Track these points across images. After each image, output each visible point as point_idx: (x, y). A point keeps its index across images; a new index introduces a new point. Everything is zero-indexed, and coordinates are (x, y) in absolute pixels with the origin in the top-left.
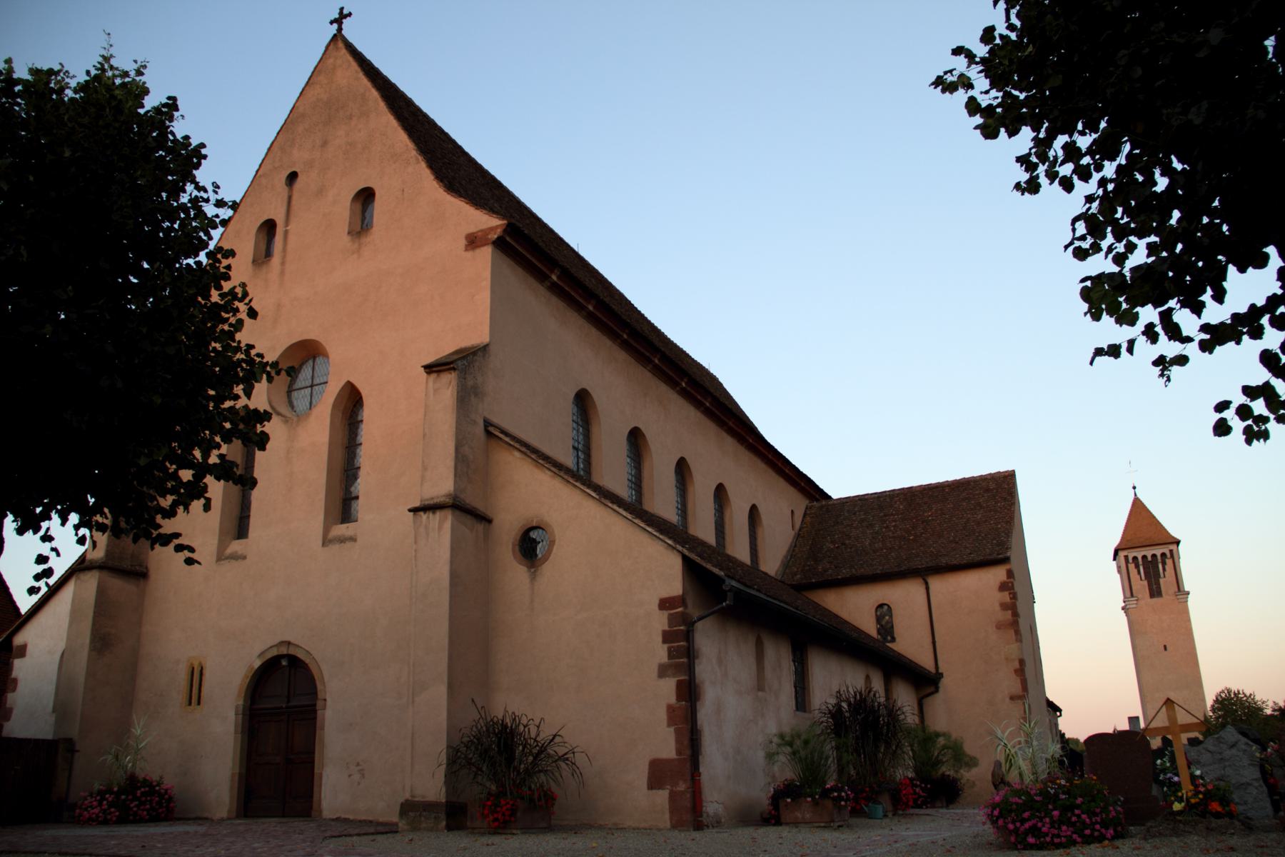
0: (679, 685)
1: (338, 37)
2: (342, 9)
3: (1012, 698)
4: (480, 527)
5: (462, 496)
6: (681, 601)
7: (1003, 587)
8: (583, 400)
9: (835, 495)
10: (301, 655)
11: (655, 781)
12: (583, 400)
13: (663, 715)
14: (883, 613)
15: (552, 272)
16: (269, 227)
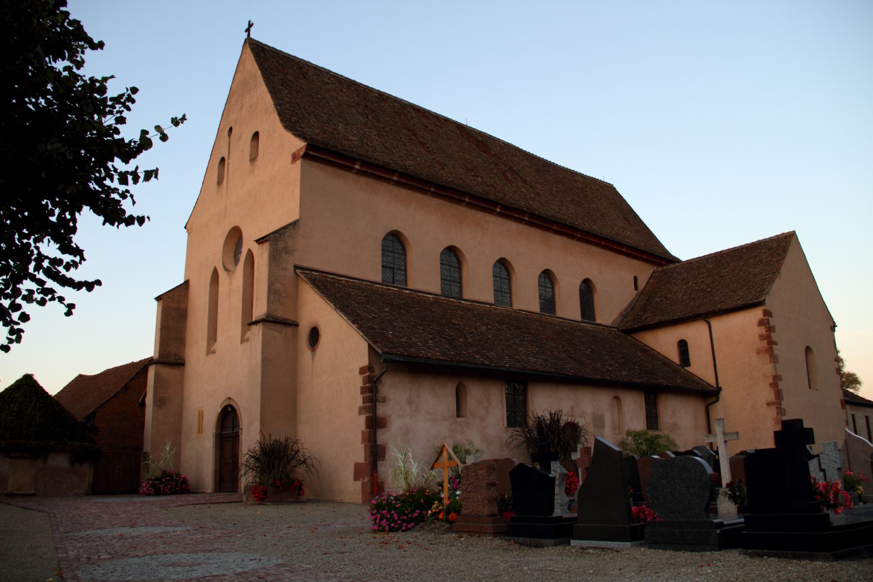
0: (367, 418)
3: (768, 404)
4: (289, 330)
5: (275, 313)
6: (370, 368)
7: (761, 323)
9: (683, 258)
10: (234, 405)
11: (356, 477)
13: (360, 437)
14: (683, 346)
15: (355, 164)
16: (223, 160)
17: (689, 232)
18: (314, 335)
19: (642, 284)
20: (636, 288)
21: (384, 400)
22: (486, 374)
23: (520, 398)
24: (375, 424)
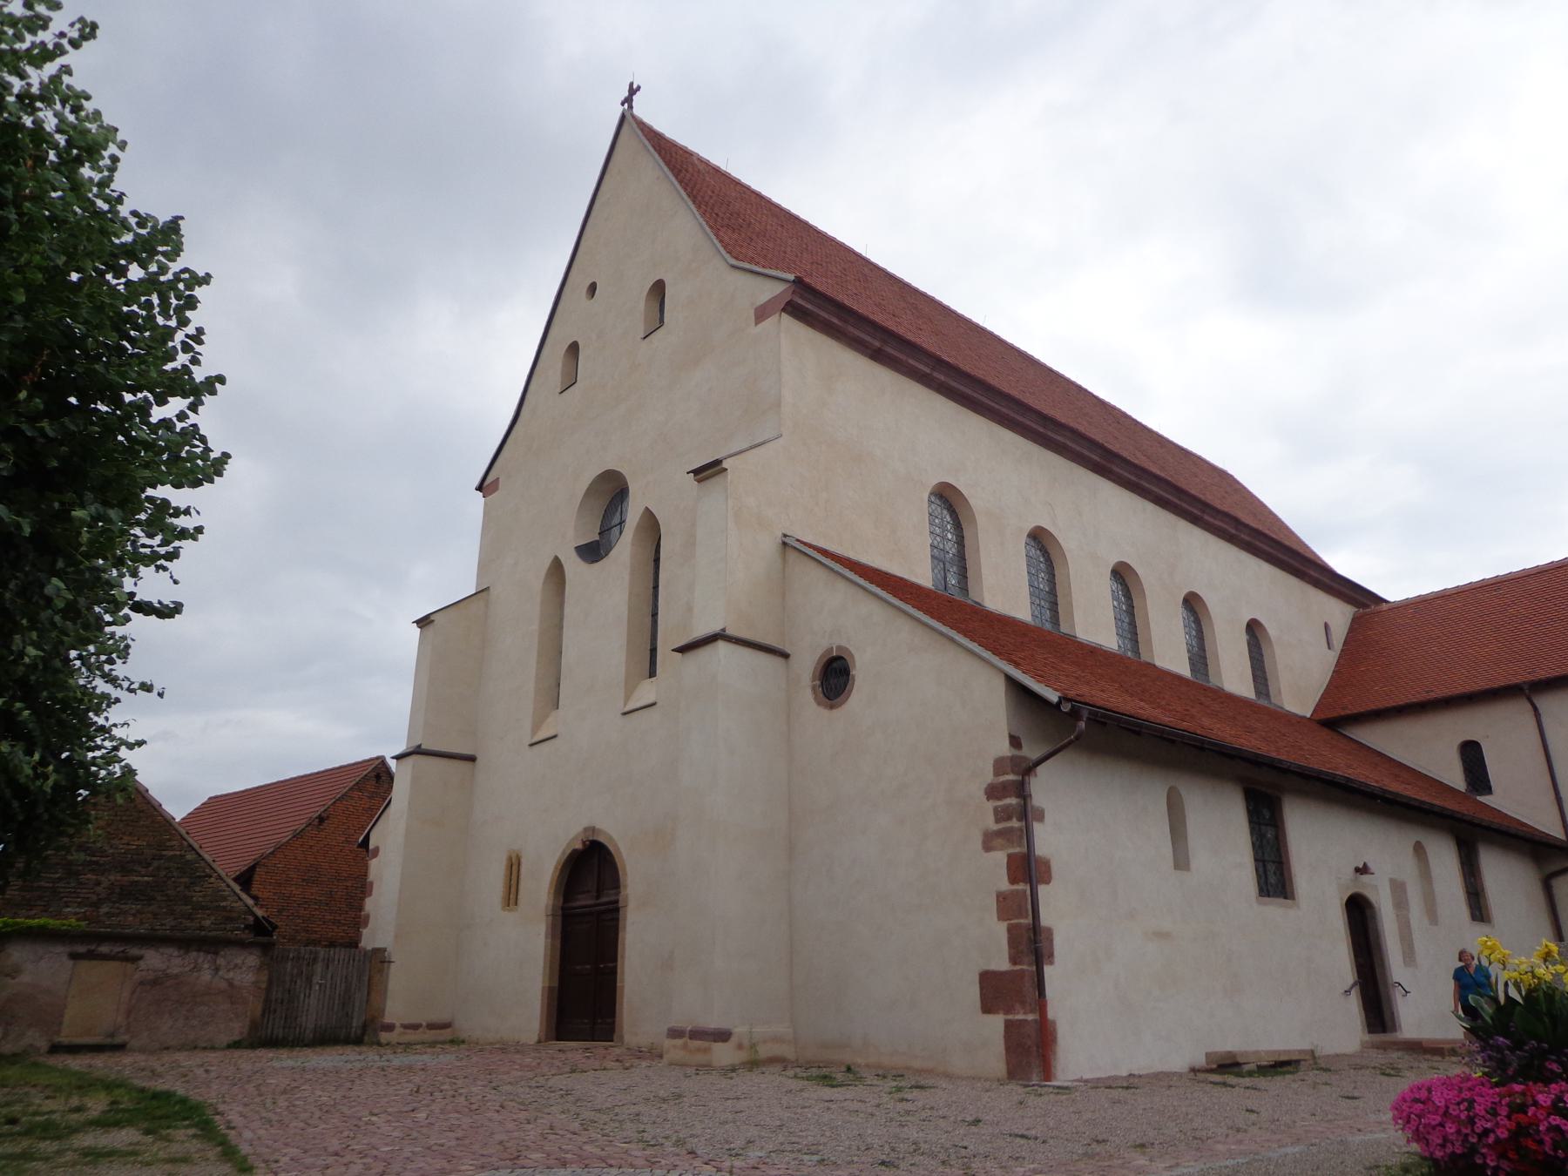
1: (626, 119)
2: (631, 85)
8: (948, 499)
12: (948, 499)
14: (1471, 754)
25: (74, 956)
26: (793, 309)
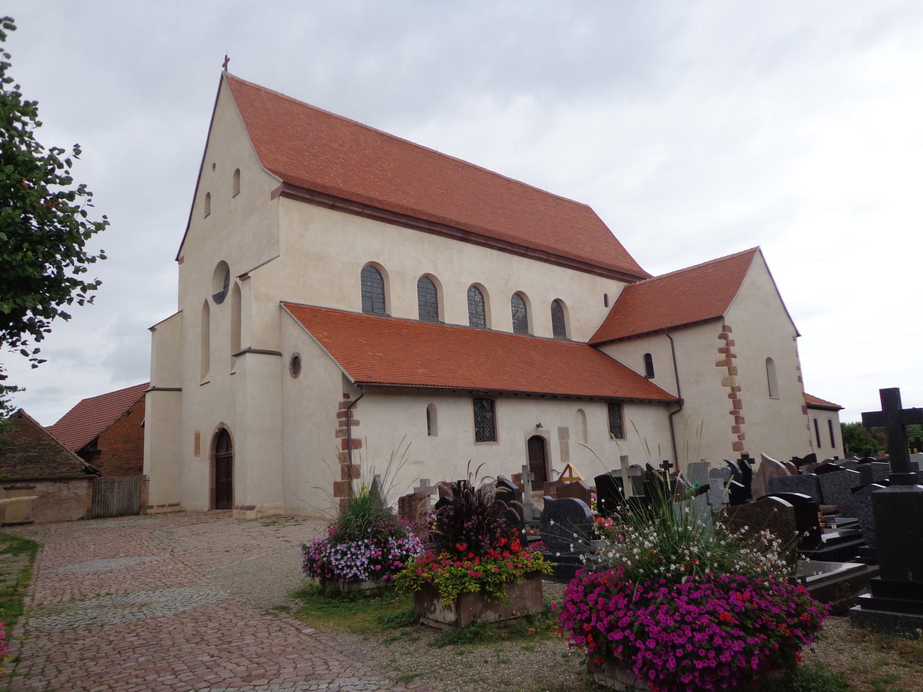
0: (343, 440)
17: (659, 252)
18: (296, 363)
19: (612, 303)
20: (606, 305)
21: (357, 423)
22: (453, 393)
23: (489, 415)
24: (350, 444)
25: (5, 489)
26: (284, 194)
